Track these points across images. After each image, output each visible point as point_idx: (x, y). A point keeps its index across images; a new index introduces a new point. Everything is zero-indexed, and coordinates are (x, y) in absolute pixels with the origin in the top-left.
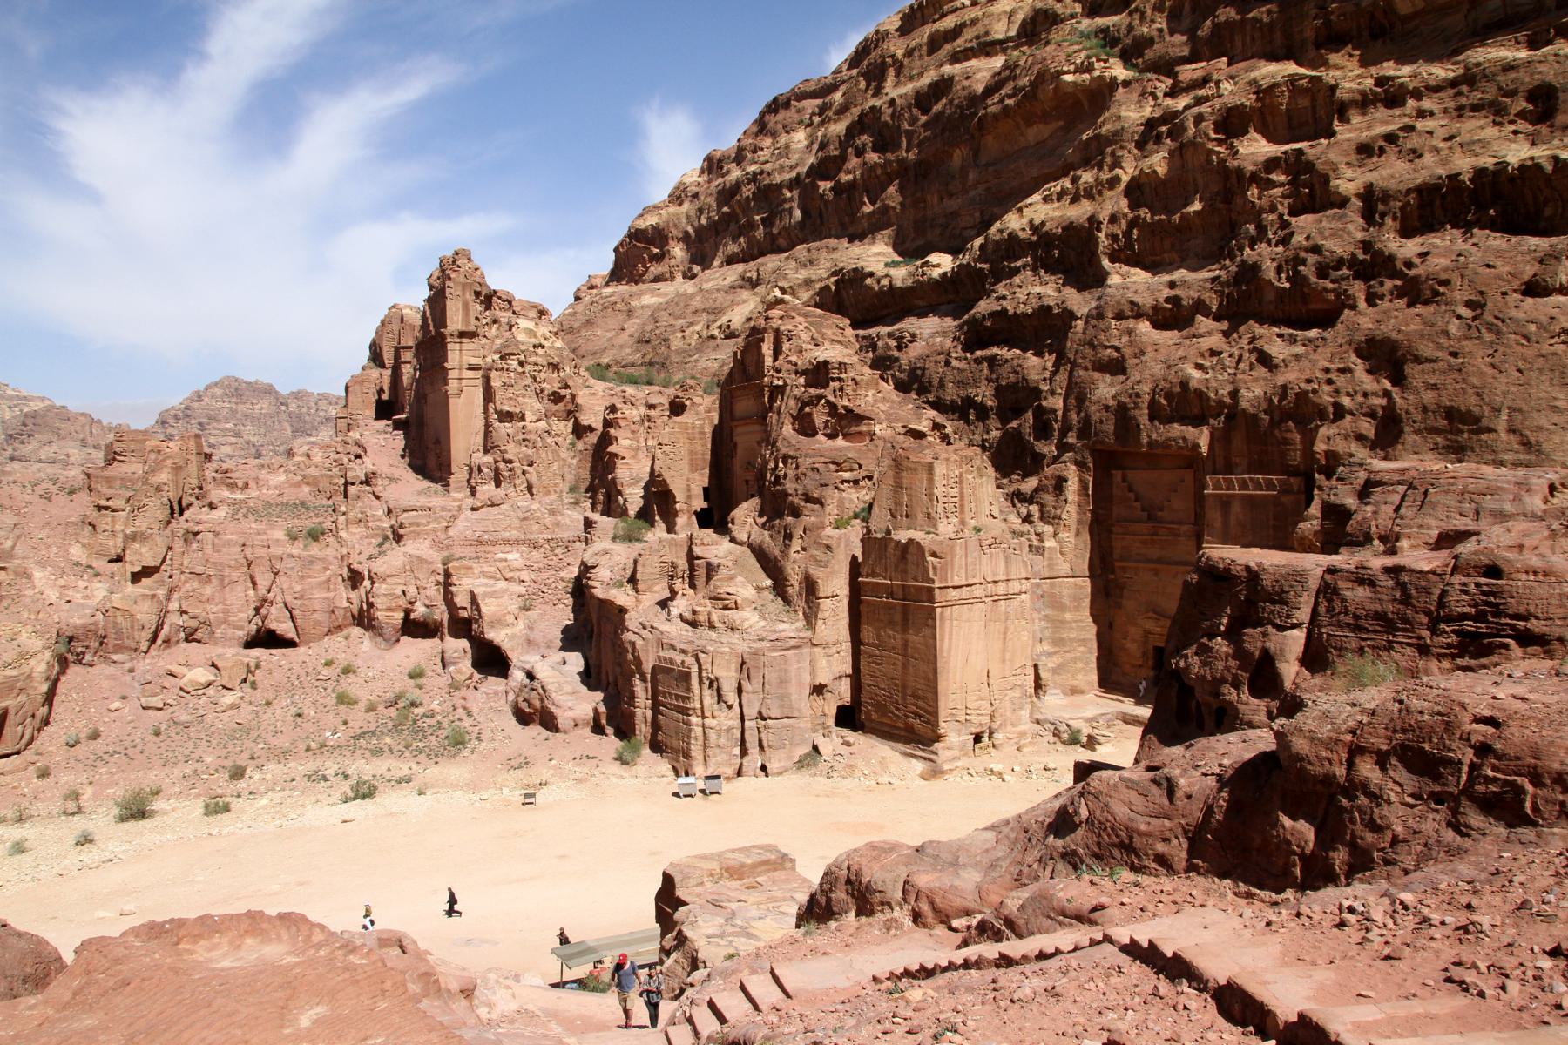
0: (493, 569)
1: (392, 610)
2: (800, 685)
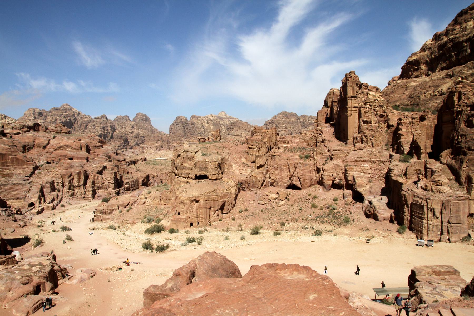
0: (360, 169)
2: (464, 213)
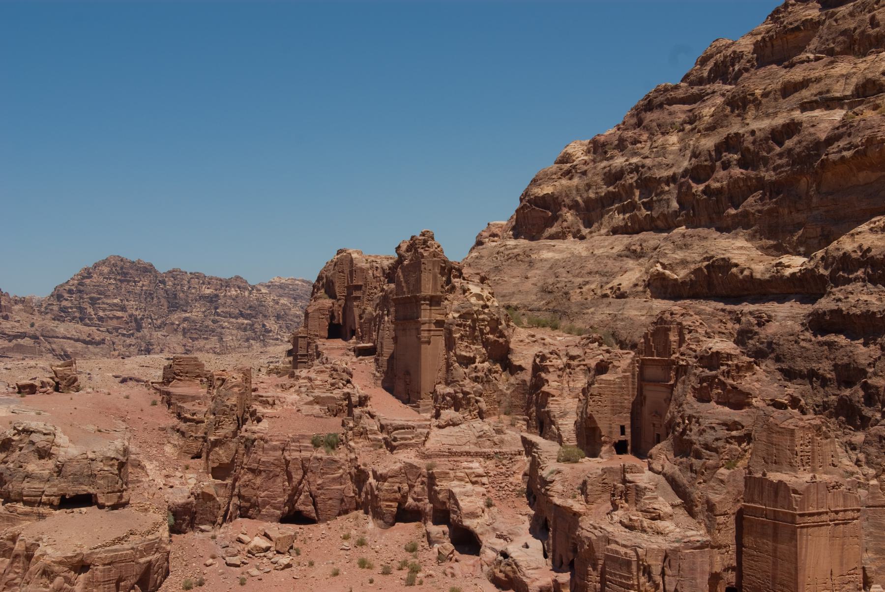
0: (462, 475)
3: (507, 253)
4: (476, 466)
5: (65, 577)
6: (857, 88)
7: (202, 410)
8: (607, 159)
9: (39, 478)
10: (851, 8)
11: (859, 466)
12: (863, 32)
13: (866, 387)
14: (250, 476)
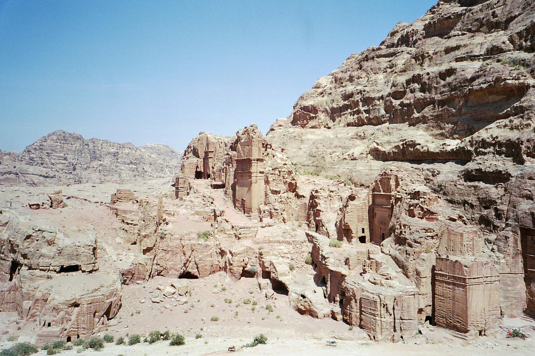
0: (277, 253)
1: (239, 267)
2: (415, 308)
3: (289, 135)
4: (283, 248)
5: (66, 311)
6: (488, 50)
7: (135, 218)
8: (343, 87)
9: (48, 257)
10: (481, 7)
11: (494, 252)
12: (489, 19)
13: (496, 210)
14: (163, 253)
